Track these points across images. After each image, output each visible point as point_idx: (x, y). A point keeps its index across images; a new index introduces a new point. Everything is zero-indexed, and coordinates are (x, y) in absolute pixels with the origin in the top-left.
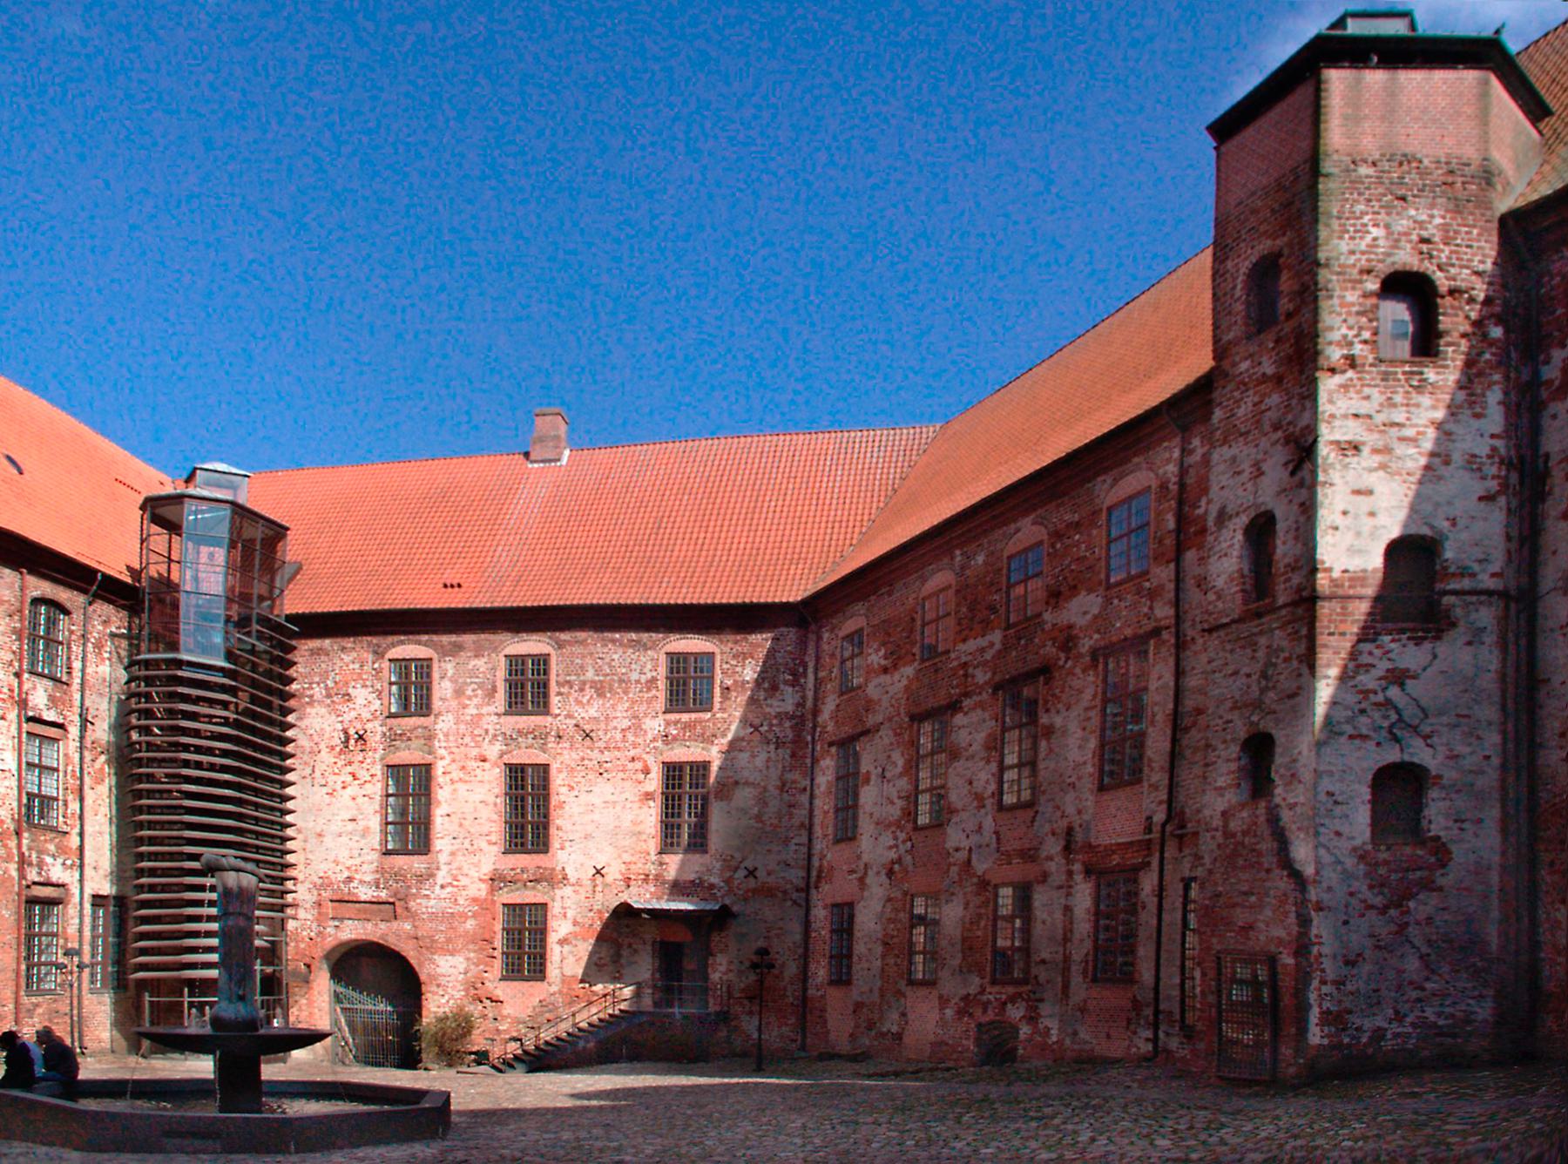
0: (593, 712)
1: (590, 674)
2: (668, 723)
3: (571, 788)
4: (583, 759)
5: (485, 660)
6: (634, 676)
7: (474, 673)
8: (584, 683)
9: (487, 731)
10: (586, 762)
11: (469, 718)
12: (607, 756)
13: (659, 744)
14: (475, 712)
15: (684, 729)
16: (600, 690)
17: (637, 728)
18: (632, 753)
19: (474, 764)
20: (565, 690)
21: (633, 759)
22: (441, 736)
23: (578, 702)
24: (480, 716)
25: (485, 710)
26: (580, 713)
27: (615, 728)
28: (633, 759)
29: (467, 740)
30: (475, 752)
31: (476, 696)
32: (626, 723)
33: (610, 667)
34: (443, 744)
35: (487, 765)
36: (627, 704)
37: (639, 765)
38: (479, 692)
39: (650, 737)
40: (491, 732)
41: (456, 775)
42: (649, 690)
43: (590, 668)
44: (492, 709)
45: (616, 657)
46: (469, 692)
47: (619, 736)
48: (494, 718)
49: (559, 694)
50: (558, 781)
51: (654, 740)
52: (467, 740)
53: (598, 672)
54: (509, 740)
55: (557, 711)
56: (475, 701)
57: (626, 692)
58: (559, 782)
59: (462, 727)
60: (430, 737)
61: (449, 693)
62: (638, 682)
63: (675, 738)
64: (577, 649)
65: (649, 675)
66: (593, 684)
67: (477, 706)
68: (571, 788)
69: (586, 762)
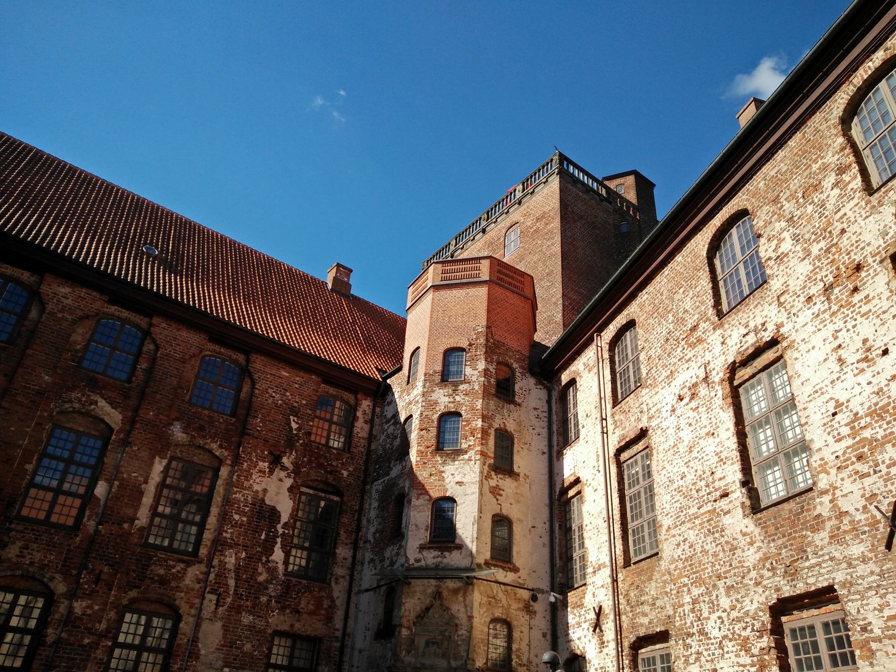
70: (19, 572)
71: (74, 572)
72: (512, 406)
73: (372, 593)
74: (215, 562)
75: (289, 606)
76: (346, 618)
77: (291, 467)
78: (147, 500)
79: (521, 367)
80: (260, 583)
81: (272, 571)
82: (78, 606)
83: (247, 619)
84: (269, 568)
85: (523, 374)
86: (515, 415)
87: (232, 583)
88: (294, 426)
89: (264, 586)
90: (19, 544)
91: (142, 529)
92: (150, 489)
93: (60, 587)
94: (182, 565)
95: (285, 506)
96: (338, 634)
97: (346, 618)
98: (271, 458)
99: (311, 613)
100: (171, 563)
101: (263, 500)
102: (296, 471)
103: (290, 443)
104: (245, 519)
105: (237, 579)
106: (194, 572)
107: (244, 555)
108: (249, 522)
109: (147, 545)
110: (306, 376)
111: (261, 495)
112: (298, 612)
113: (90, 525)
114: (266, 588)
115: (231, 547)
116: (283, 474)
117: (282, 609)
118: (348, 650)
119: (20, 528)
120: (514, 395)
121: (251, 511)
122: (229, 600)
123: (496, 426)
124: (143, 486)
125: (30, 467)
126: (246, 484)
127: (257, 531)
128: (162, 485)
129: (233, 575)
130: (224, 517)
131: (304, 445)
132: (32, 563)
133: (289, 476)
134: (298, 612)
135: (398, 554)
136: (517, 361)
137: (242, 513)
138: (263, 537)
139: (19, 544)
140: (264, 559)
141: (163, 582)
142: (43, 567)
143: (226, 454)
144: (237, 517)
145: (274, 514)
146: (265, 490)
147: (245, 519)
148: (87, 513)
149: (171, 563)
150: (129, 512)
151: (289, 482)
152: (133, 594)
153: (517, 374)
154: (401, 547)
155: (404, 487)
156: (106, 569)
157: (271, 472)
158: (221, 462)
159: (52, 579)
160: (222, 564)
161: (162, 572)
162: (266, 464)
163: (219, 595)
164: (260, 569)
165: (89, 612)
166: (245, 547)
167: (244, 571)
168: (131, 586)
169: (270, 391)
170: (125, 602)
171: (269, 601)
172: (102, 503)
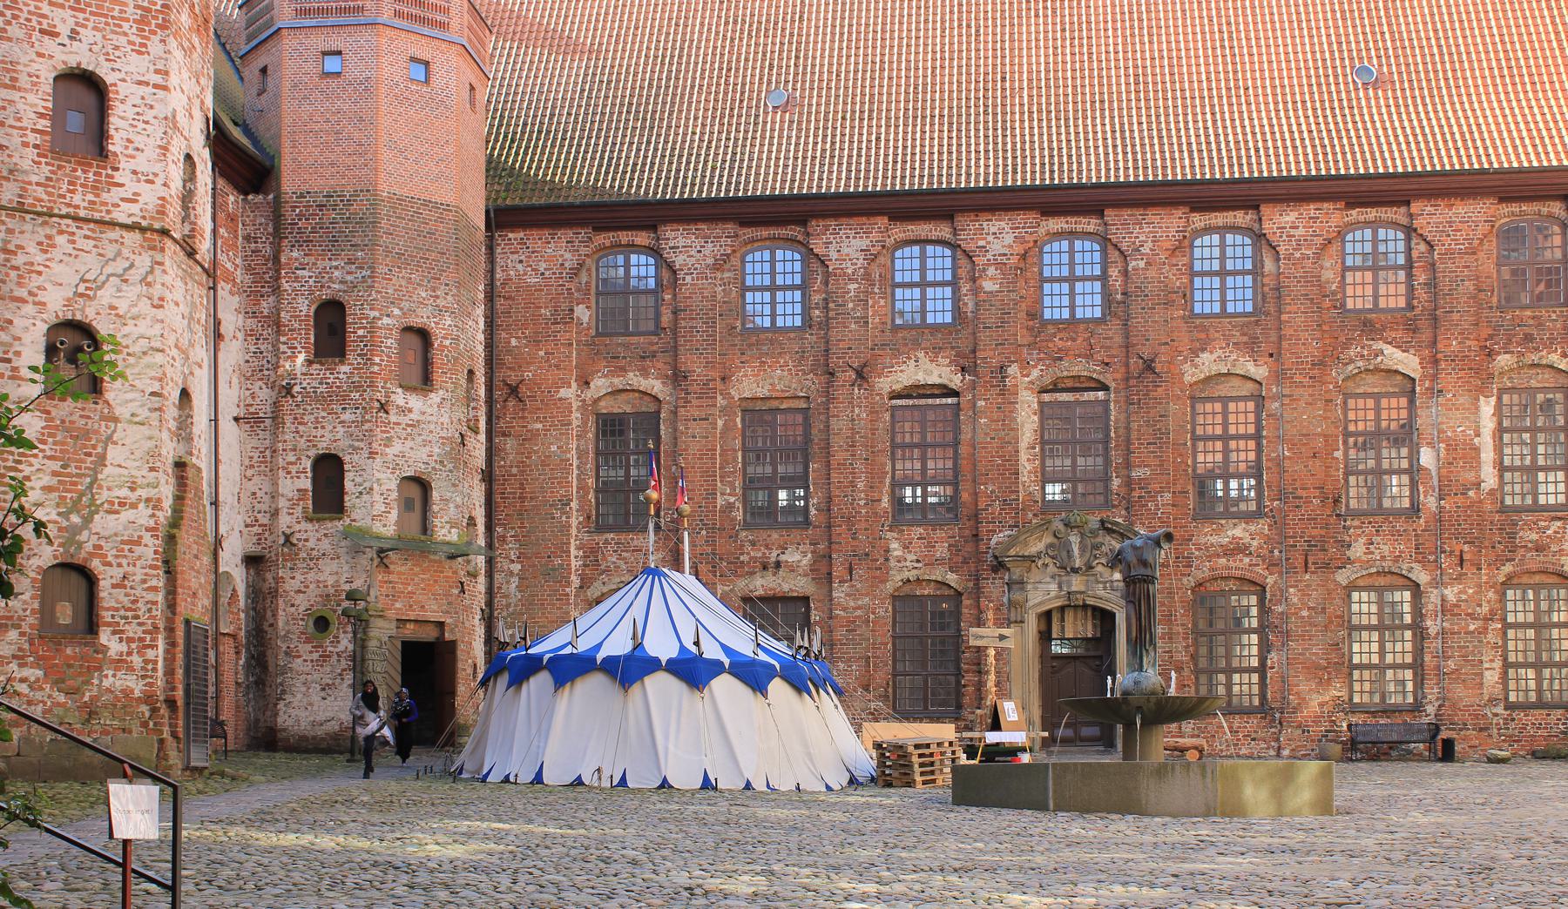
70: (1374, 570)
71: (1432, 558)
78: (1487, 455)
82: (1451, 593)
90: (1362, 540)
91: (1492, 492)
92: (1486, 442)
93: (1422, 577)
94: (1559, 524)
100: (1542, 524)
109: (1504, 510)
113: (1430, 502)
119: (1356, 523)
124: (1476, 440)
125: (1339, 454)
128: (1500, 430)
132: (1383, 558)
139: (1362, 540)
141: (1539, 548)
142: (1396, 559)
148: (1421, 489)
149: (1542, 524)
150: (1470, 476)
152: (1508, 568)
156: (1466, 548)
159: (1410, 570)
161: (1534, 536)
165: (1464, 597)
168: (1501, 561)
170: (1501, 579)
172: (1434, 473)
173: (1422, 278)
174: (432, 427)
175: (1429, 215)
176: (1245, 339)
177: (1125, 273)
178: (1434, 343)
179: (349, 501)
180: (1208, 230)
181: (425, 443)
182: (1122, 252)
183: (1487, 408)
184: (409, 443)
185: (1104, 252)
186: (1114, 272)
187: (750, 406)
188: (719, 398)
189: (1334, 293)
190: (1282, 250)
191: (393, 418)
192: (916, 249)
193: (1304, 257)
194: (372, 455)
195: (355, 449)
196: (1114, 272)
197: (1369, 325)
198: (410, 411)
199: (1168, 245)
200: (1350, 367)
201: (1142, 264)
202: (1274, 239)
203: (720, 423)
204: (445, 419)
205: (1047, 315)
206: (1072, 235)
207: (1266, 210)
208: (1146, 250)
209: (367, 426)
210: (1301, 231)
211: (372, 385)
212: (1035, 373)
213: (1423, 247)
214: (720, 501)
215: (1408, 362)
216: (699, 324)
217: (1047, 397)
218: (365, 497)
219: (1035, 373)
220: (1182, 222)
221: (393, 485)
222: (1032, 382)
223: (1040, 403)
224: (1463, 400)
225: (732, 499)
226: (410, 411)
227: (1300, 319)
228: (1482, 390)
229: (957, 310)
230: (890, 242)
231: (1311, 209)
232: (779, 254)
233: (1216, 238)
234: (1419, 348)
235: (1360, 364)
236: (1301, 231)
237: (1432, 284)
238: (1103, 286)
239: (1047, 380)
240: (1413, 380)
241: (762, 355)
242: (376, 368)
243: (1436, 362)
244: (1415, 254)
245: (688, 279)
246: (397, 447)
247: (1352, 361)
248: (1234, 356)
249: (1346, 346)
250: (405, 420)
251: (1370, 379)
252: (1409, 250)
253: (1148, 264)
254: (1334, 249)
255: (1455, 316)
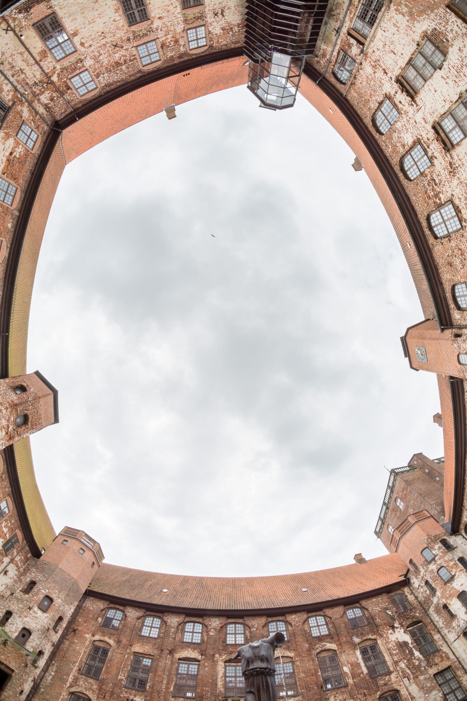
0: (117, 55)
1: (124, 67)
2: (83, 66)
3: (114, 21)
4: (114, 36)
5: (168, 57)
6: (106, 75)
7: (172, 50)
8: (125, 64)
9: (161, 30)
10: (112, 35)
11: (170, 33)
12: (103, 42)
13: (82, 57)
14: (168, 36)
15: (76, 68)
16: (118, 64)
17: (96, 59)
18: (92, 48)
19: (164, 15)
20: (132, 58)
21: (90, 46)
22: (181, 22)
23: (125, 56)
24: (166, 35)
25: (164, 38)
26: (123, 52)
27: (105, 54)
28: (90, 46)
29: (169, 24)
30: (164, 20)
31: (169, 42)
32: (101, 58)
33: (117, 73)
34: (179, 19)
35: (158, 16)
36: (104, 64)
37: (86, 45)
38: (168, 44)
39: (88, 58)
40: (159, 31)
41: (171, 8)
42: (98, 73)
43: (125, 69)
44: (161, 40)
45: (116, 77)
46: (172, 43)
47: (102, 52)
48: (159, 36)
49: (134, 55)
50: (122, 21)
51: (85, 58)
52: (169, 24)
53: (121, 70)
54: (151, 30)
55: (133, 49)
56: (169, 40)
57: (106, 68)
58: (122, 21)
59: (172, 29)
60: (185, 21)
61: (181, 40)
62: (103, 74)
63: (77, 62)
64: (132, 73)
65: (100, 78)
66: (121, 65)
67: (167, 39)
68: (114, 21)
69: (112, 35)
72: (455, 549)
73: (458, 640)
74: (398, 669)
75: (432, 665)
76: (454, 654)
77: (399, 626)
79: (447, 536)
80: (418, 665)
81: (419, 659)
83: (422, 678)
84: (417, 659)
85: (449, 538)
86: (458, 551)
87: (408, 671)
88: (390, 613)
89: (420, 665)
95: (407, 638)
96: (455, 660)
97: (454, 654)
98: (391, 628)
99: (441, 661)
101: (399, 642)
102: (402, 626)
103: (393, 619)
104: (397, 651)
105: (409, 669)
106: (393, 676)
107: (406, 661)
108: (400, 651)
110: (381, 596)
111: (397, 641)
112: (437, 664)
114: (421, 665)
115: (400, 662)
116: (398, 630)
117: (431, 667)
118: (462, 662)
120: (453, 546)
121: (398, 647)
122: (412, 676)
123: (457, 559)
126: (389, 641)
127: (404, 652)
129: (407, 669)
130: (391, 654)
131: (398, 616)
133: (401, 629)
134: (437, 664)
135: (458, 622)
136: (444, 536)
137: (396, 649)
138: (407, 652)
140: (413, 658)
143: (375, 636)
144: (394, 652)
145: (406, 643)
146: (397, 638)
147: (397, 651)
151: (402, 630)
153: (448, 539)
154: (458, 619)
155: (443, 602)
157: (394, 632)
158: (375, 640)
160: (401, 668)
162: (391, 630)
163: (407, 677)
164: (414, 661)
166: (404, 658)
167: (410, 665)
169: (374, 608)
171: (425, 668)
173: (331, 626)
174: (41, 621)
175: (329, 612)
176: (286, 647)
177: (250, 632)
178: (339, 640)
179: (7, 624)
180: (272, 621)
181: (36, 623)
182: (249, 627)
183: (358, 653)
184: (31, 621)
185: (244, 627)
186: (247, 632)
187: (137, 654)
188: (128, 650)
189: (309, 633)
190: (293, 624)
191: (31, 612)
192: (192, 624)
193: (299, 625)
194: (20, 617)
195: (17, 613)
196: (247, 632)
197: (320, 639)
198: (37, 613)
199: (262, 625)
200: (318, 650)
201: (255, 629)
202: (290, 622)
203: (126, 656)
204: (46, 621)
205: (228, 642)
206: (235, 623)
207: (287, 616)
208: (256, 626)
209: (23, 610)
210: (297, 619)
211: (30, 602)
212: (224, 657)
213: (329, 619)
214: (119, 677)
215: (333, 646)
216: (128, 630)
217: (227, 664)
218: (11, 625)
219: (224, 657)
220: (265, 620)
221: (21, 627)
222: (223, 660)
223: (225, 665)
224: (351, 652)
225: (123, 678)
226: (37, 613)
227: (301, 640)
228: (355, 649)
229: (202, 640)
230: (186, 621)
231: (299, 614)
232: (155, 619)
233: (275, 623)
234: (335, 642)
235: (320, 649)
236: (296, 620)
237: (334, 626)
238: (244, 636)
239: (228, 659)
240: (335, 651)
241: (143, 642)
242: (34, 599)
243: (341, 644)
244: (327, 621)
245: (129, 619)
246: (28, 619)
247: (317, 649)
248: (283, 651)
249: (315, 645)
250: (34, 614)
251: (324, 653)
252: (325, 620)
253: (257, 629)
254: (306, 622)
255: (342, 633)
